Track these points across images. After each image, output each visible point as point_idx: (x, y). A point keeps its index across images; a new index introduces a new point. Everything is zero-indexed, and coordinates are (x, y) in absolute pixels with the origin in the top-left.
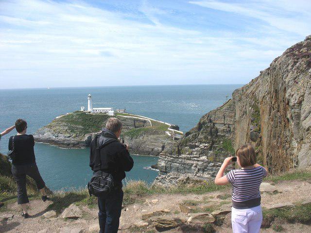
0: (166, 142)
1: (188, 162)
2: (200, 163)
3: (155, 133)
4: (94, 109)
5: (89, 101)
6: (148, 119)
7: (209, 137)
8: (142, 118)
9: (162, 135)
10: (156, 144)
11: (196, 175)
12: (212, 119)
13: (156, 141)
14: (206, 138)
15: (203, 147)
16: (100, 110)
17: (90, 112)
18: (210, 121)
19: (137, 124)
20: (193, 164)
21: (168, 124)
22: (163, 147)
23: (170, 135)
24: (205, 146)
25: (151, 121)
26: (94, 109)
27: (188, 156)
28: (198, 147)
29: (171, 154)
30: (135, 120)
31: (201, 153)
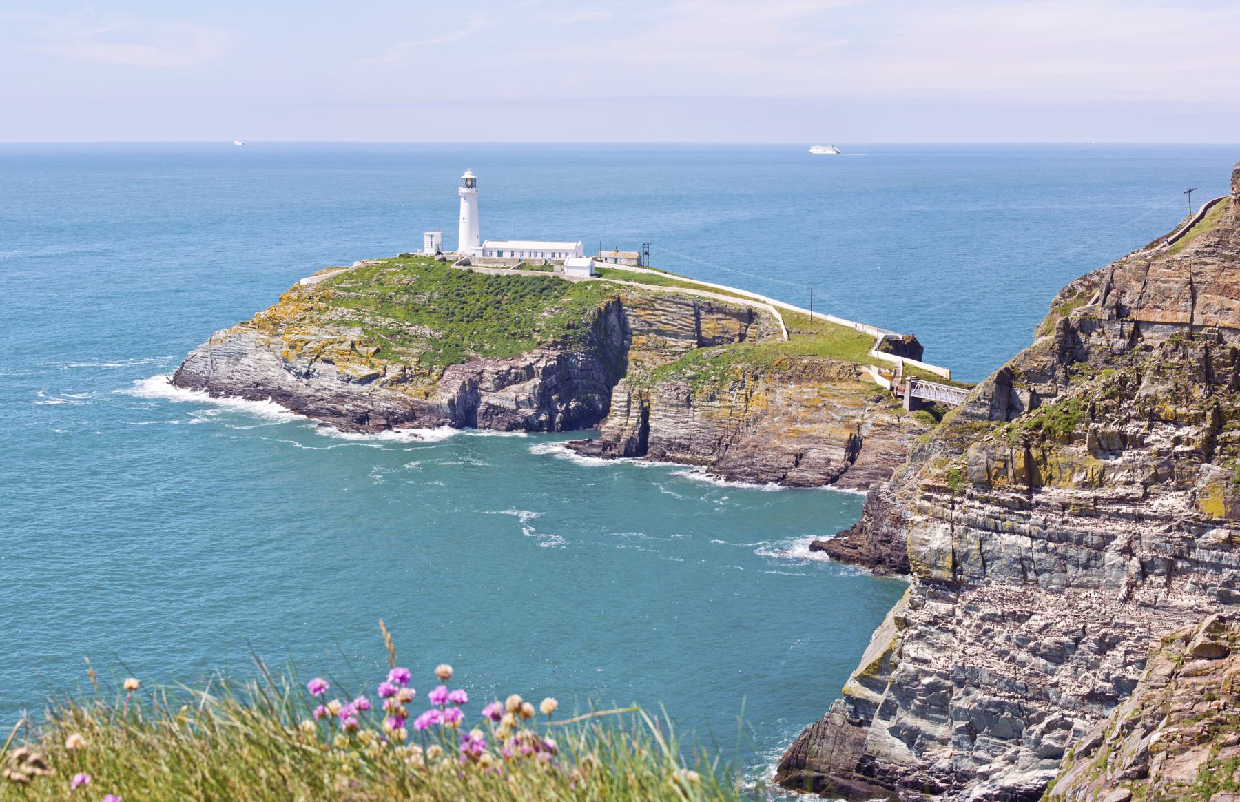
0: (870, 419)
1: (1085, 525)
3: (813, 373)
4: (489, 245)
5: (464, 207)
6: (768, 305)
7: (1199, 392)
8: (739, 298)
9: (844, 385)
10: (817, 429)
11: (1128, 598)
12: (1126, 301)
13: (816, 415)
14: (1177, 396)
15: (1167, 444)
16: (517, 250)
17: (467, 263)
18: (1120, 312)
19: (710, 326)
21: (871, 331)
22: (854, 446)
23: (886, 384)
24: (1178, 441)
25: (776, 308)
26: (489, 245)
27: (1084, 493)
28: (1139, 443)
29: (986, 485)
30: (700, 309)
31: (1157, 479)
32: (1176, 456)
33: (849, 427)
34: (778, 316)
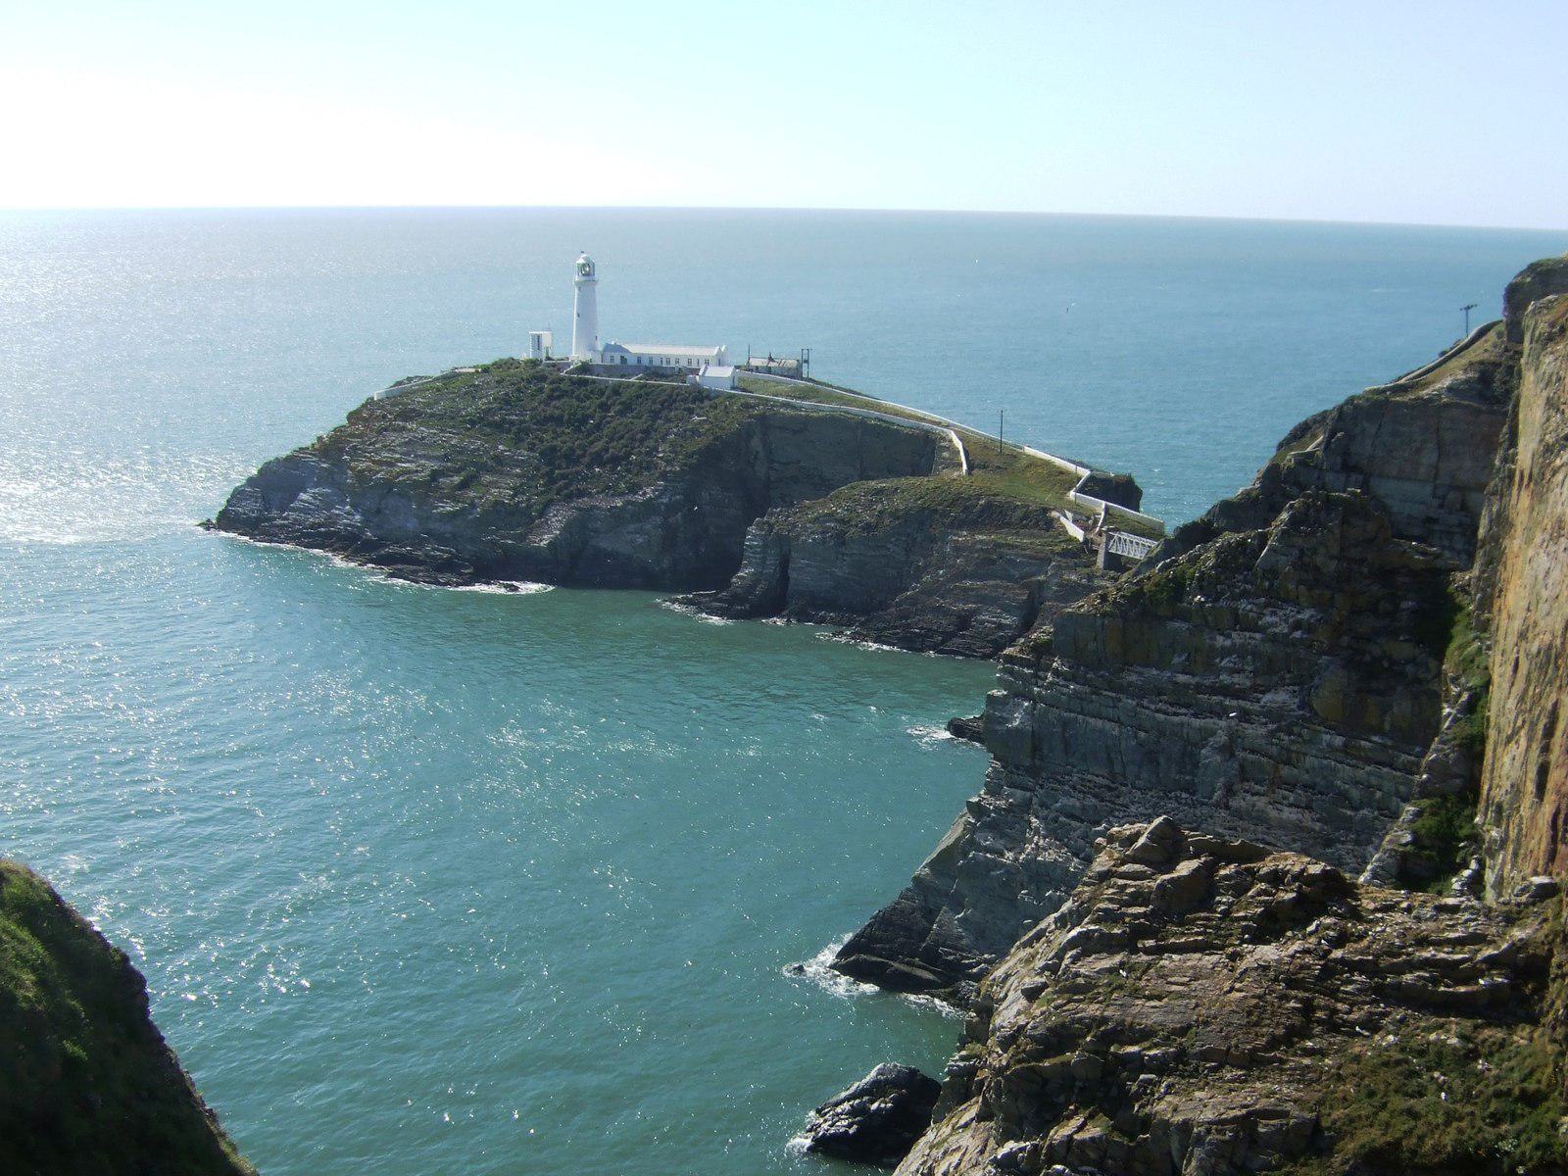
1: (1183, 718)
2: (1256, 731)
15: (1283, 629)
20: (1207, 734)
27: (1181, 678)
32: (1294, 643)
33: (1027, 586)
34: (959, 444)
